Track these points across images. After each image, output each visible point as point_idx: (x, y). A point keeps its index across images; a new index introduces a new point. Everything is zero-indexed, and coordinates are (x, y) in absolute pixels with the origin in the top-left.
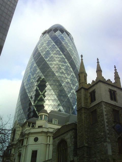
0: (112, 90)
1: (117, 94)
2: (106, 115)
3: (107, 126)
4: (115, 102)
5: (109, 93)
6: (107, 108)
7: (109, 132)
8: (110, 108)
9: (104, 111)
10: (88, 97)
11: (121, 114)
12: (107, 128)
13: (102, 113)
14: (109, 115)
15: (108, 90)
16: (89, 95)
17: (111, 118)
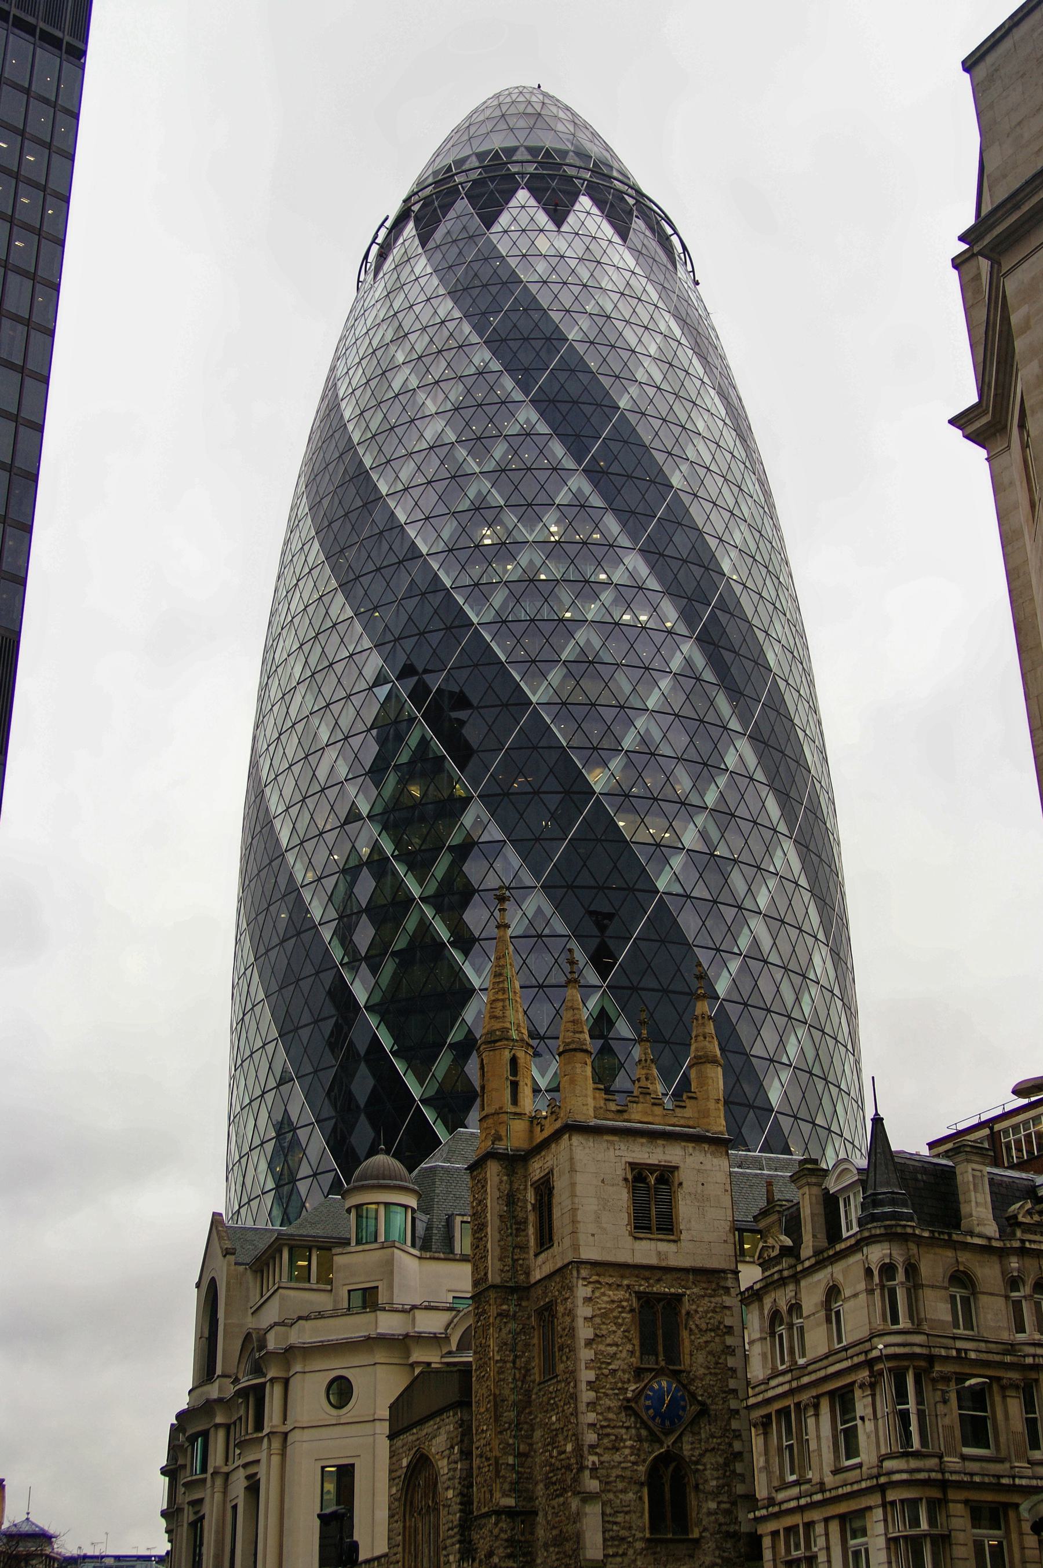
0: (652, 1168)
1: (681, 1184)
2: (589, 1343)
3: (592, 1405)
4: (663, 1247)
5: (622, 1196)
6: (604, 1294)
7: (601, 1437)
8: (621, 1294)
9: (580, 1322)
10: (530, 1207)
11: (688, 1313)
12: (591, 1417)
13: (572, 1332)
14: (609, 1341)
15: (620, 1171)
16: (531, 1196)
17: (624, 1354)
